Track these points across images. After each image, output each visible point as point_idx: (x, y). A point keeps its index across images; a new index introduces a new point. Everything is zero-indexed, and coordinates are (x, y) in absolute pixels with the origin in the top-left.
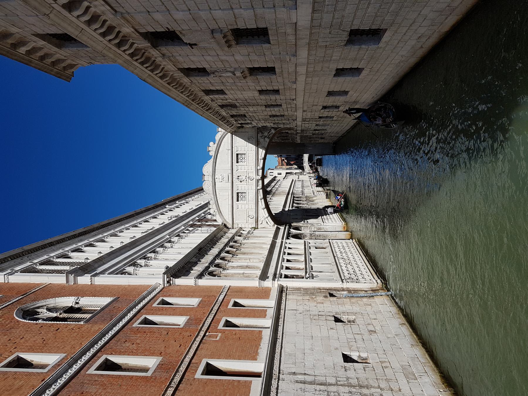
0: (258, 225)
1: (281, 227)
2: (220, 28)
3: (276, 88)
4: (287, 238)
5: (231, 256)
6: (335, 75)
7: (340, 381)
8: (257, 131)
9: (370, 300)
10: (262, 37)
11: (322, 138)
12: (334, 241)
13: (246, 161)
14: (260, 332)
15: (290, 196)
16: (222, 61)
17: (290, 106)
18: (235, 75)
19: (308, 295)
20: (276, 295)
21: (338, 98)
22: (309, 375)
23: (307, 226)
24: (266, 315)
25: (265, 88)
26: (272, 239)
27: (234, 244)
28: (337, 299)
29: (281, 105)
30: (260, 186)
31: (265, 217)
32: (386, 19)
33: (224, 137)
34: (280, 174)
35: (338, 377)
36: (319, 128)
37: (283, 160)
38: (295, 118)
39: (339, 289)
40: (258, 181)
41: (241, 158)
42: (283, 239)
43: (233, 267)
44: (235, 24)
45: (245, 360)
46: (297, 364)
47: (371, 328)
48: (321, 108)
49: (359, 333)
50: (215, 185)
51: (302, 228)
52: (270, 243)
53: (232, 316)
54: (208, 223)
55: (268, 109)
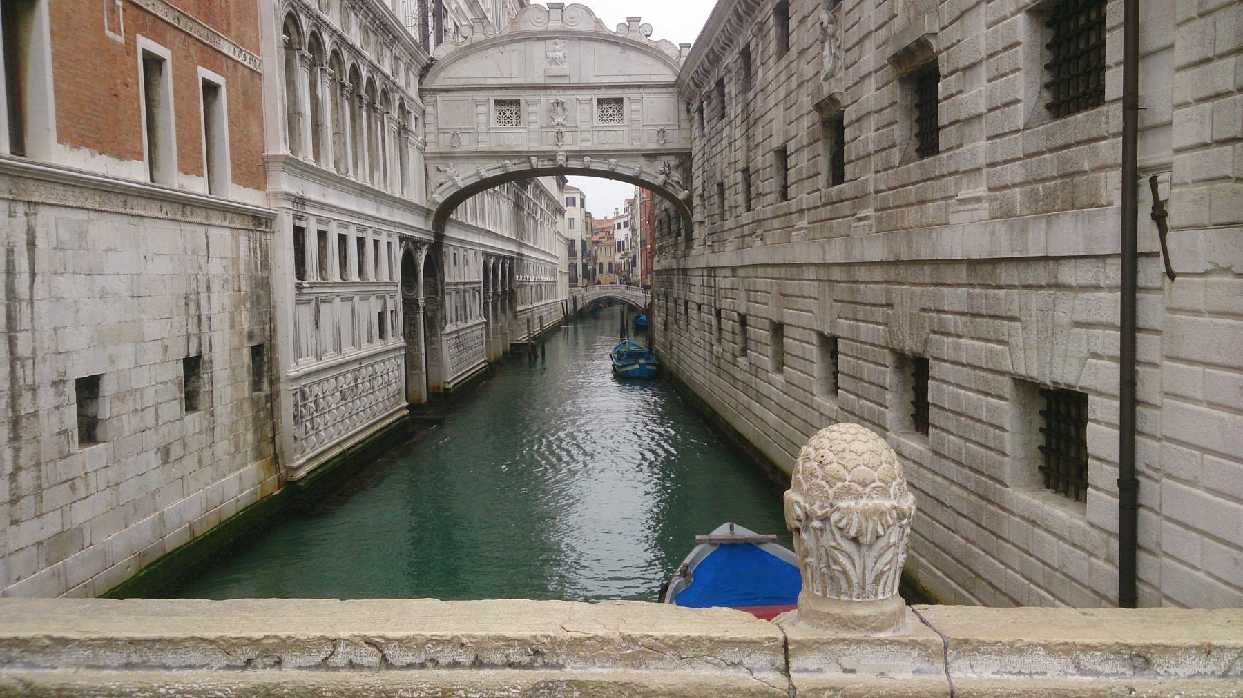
0: (435, 158)
1: (430, 223)
2: (942, 29)
3: (792, 191)
4: (402, 238)
5: (346, 81)
6: (821, 335)
7: (23, 366)
8: (683, 154)
9: (249, 449)
10: (914, 145)
11: (666, 324)
12: (401, 362)
13: (605, 124)
14: (139, 157)
15: (513, 248)
16: (861, 41)
17: (746, 230)
18: (826, 79)
19: (252, 288)
20: (244, 201)
21: (769, 351)
22: (31, 286)
23: (437, 295)
24: (186, 174)
25: (793, 165)
26: (398, 194)
27: (379, 92)
29: (749, 209)
30: (540, 163)
31: (458, 179)
32: (951, 437)
33: (665, 63)
34: (571, 227)
35: (34, 364)
36: (693, 313)
38: (716, 250)
39: (274, 372)
40: (552, 159)
41: (611, 112)
43: (313, 86)
44: (951, 69)
45: (57, 110)
46: (59, 252)
47: (176, 451)
48: (743, 311)
49: (160, 419)
50: (539, 39)
51: (432, 280)
52: (389, 193)
54: (431, 19)
55: (739, 176)
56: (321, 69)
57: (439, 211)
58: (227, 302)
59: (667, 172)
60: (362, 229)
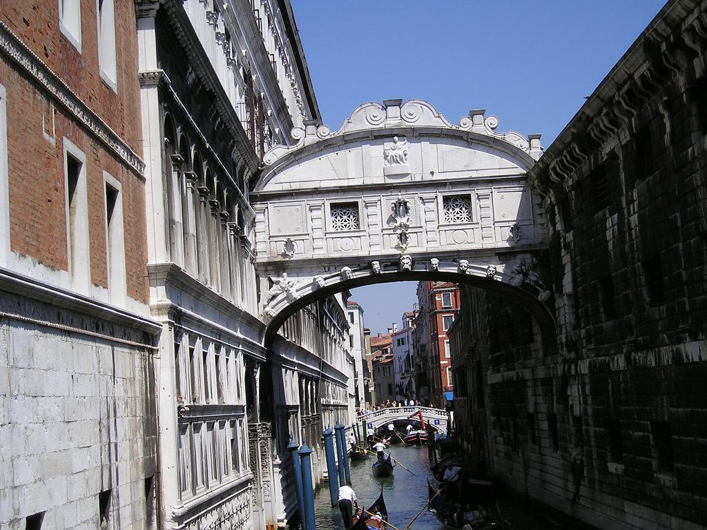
8: (538, 251)
13: (452, 223)
24: (96, 285)
28: (142, 502)
31: (293, 290)
37: (385, 351)
41: (457, 210)
42: (244, 342)
50: (376, 138)
53: (90, 182)
56: (186, 174)
57: (271, 324)
58: (127, 429)
59: (524, 271)
60: (218, 349)
